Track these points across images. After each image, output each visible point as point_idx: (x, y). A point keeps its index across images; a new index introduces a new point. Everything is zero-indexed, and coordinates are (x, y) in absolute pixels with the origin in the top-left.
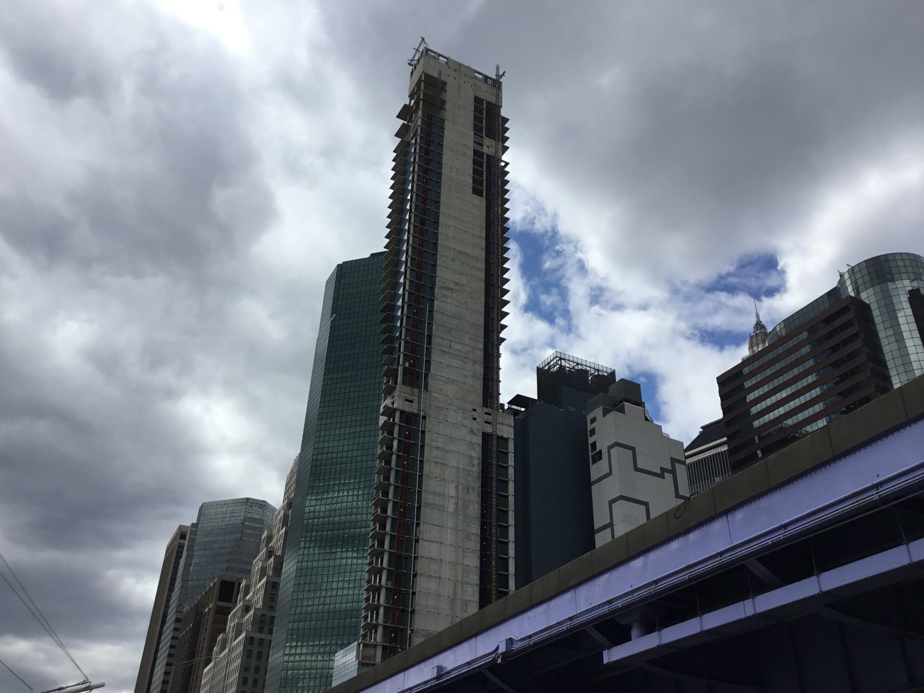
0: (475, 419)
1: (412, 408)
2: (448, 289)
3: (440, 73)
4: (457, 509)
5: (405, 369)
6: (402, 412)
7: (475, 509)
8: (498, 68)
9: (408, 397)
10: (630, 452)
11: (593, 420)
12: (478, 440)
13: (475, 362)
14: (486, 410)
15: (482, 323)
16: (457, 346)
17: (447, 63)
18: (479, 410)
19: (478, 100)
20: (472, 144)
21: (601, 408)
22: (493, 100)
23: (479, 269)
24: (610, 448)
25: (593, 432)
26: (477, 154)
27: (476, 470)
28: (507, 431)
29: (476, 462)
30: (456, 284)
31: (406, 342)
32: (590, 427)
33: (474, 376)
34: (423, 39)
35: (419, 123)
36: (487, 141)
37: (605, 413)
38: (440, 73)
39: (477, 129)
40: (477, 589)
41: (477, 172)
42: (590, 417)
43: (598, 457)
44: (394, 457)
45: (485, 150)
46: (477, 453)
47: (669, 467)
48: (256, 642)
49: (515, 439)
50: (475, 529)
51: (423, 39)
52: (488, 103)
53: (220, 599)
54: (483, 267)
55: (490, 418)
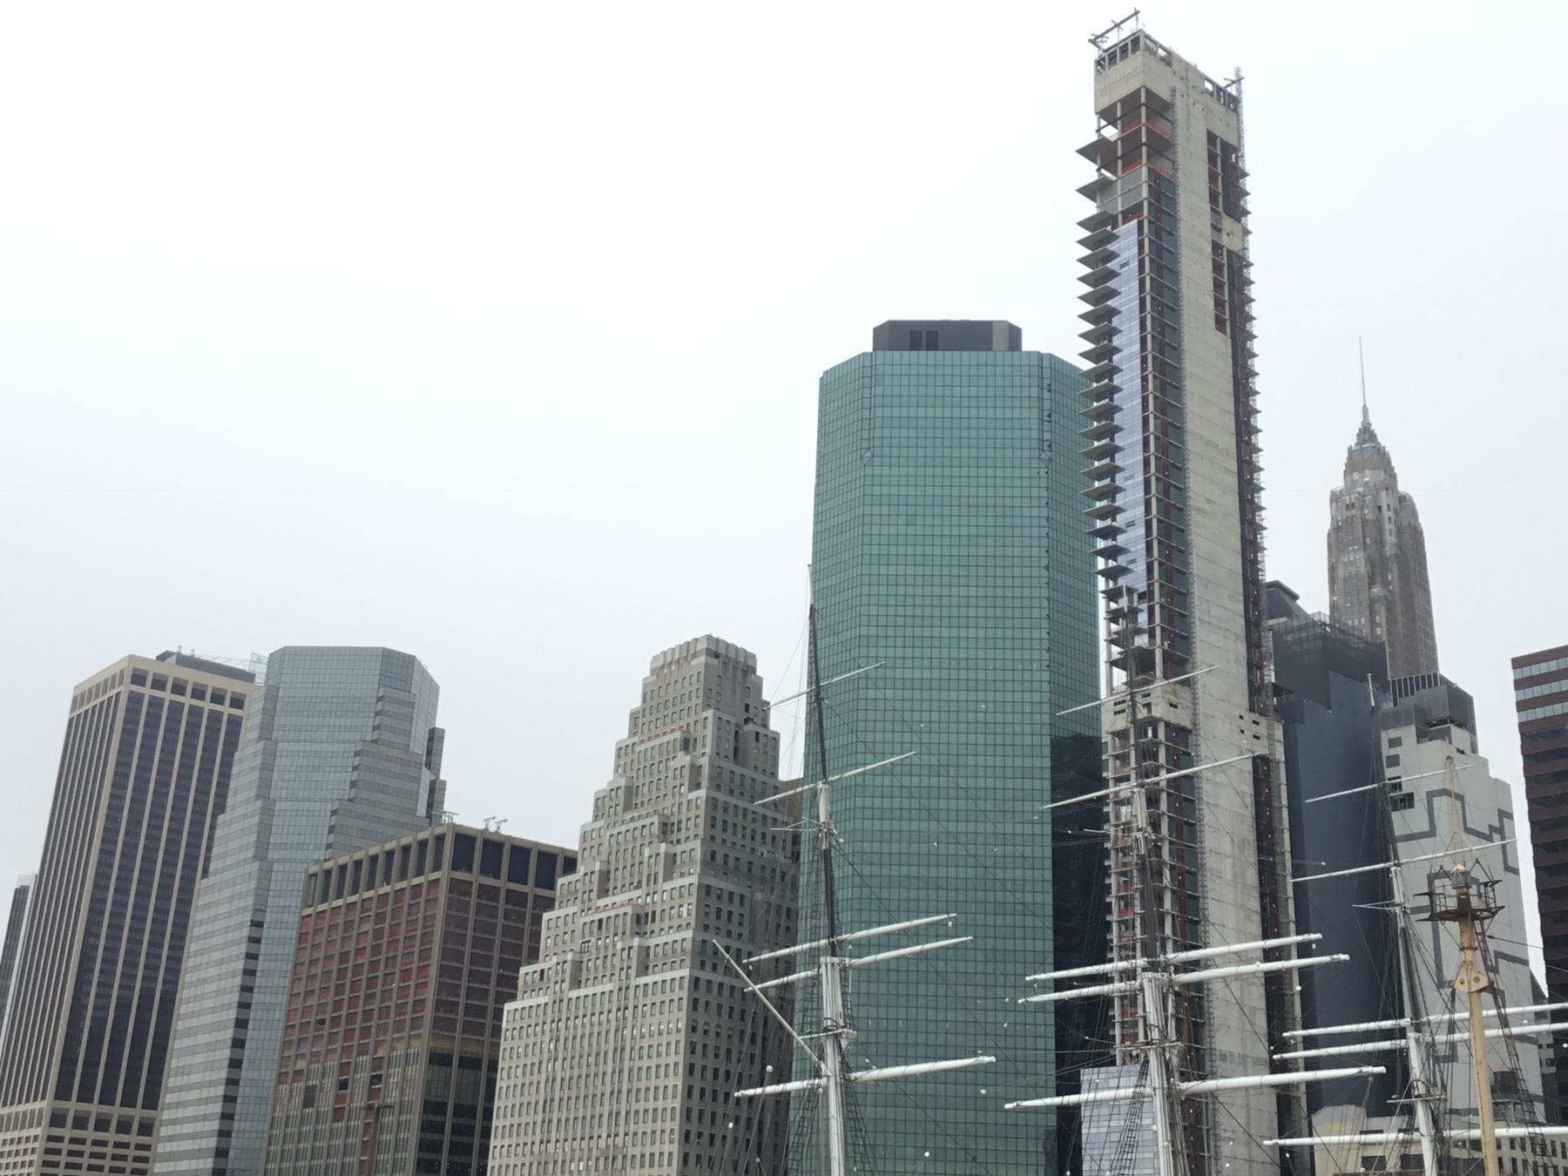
0: (1257, 737)
1: (1182, 718)
2: (1201, 511)
3: (1174, 91)
4: (1234, 875)
5: (1164, 652)
6: (1167, 724)
7: (1252, 876)
8: (1238, 71)
9: (1174, 700)
10: (1459, 803)
11: (1395, 743)
12: (1249, 767)
13: (1236, 636)
14: (1254, 716)
15: (1240, 571)
16: (1215, 611)
17: (1162, 59)
18: (1247, 715)
19: (1211, 138)
20: (1208, 230)
21: (1413, 728)
22: (1233, 141)
23: (1227, 471)
24: (1431, 795)
25: (1394, 761)
26: (1217, 247)
27: (1249, 813)
28: (1280, 754)
29: (1249, 800)
30: (1208, 501)
31: (1162, 607)
32: (1386, 751)
33: (1237, 660)
34: (1136, 13)
35: (1145, 193)
36: (1227, 223)
37: (1422, 736)
38: (1174, 91)
39: (1213, 198)
40: (1262, 991)
41: (1218, 286)
42: (1385, 736)
43: (1408, 801)
44: (1164, 795)
45: (1226, 241)
46: (1248, 788)
47: (1497, 825)
48: (702, 985)
49: (1286, 762)
50: (1255, 905)
51: (1136, 13)
52: (1225, 144)
53: (455, 867)
54: (1235, 468)
55: (1262, 730)
